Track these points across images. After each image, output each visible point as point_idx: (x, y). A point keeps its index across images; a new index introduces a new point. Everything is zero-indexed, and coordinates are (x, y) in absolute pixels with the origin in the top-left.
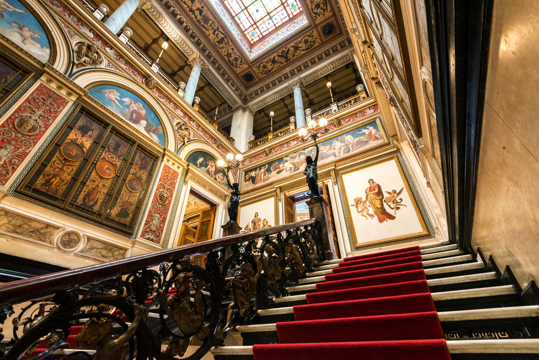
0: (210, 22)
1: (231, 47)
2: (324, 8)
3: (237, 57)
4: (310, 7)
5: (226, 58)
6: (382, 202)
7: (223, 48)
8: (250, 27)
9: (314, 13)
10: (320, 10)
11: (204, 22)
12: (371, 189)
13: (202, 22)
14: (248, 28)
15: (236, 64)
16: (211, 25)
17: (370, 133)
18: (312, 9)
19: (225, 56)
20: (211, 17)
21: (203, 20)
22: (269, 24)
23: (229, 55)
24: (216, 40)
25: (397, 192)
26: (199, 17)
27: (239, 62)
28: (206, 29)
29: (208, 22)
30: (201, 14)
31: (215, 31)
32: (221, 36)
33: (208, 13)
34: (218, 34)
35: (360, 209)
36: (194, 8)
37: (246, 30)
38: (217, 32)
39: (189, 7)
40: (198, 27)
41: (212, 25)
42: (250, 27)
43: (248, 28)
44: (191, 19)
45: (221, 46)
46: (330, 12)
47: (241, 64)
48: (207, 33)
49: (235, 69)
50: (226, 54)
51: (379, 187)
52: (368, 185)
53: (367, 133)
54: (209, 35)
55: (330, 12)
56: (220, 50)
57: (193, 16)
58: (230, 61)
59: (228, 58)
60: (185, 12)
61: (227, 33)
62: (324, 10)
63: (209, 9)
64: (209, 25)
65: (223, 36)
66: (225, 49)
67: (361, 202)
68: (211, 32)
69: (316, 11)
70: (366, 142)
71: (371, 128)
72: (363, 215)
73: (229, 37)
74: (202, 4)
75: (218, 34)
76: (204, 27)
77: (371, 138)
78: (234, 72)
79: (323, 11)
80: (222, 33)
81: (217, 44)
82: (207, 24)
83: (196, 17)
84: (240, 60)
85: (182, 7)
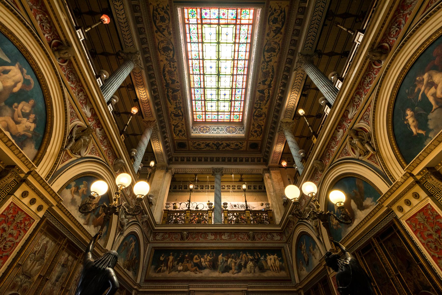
0: (264, 71)
1: (268, 38)
2: (157, 13)
3: (271, 23)
4: (171, 23)
5: (282, 30)
7: (276, 43)
8: (243, 24)
9: (168, 15)
10: (161, 12)
11: (269, 73)
13: (270, 75)
14: (245, 24)
15: (279, 15)
16: (267, 68)
18: (169, 20)
19: (281, 33)
20: (260, 73)
21: (268, 76)
22: (224, 14)
23: (278, 31)
24: (275, 54)
26: (269, 79)
27: (276, 15)
28: (273, 68)
29: (266, 72)
30: (266, 80)
31: (268, 62)
32: (267, 55)
33: (259, 77)
34: (268, 58)
36: (266, 87)
37: (249, 24)
38: (267, 60)
39: (269, 90)
40: (277, 74)
41: (265, 68)
42: (243, 24)
43: (245, 24)
44: (276, 82)
45: (276, 46)
46: (151, 4)
47: (275, 10)
48: (275, 65)
49: (287, 10)
50: (279, 35)
54: (276, 62)
55: (151, 4)
56: (280, 42)
57: (272, 82)
58: (283, 24)
59: (281, 29)
60: (274, 89)
61: (260, 53)
62: (157, 11)
63: (257, 80)
64: (268, 70)
65: (266, 53)
66: (275, 40)
68: (272, 63)
69: (166, 16)
73: (261, 49)
74: (258, 85)
75: (268, 58)
76: (273, 71)
78: (291, 7)
79: (159, 10)
80: (264, 56)
81: (277, 50)
82: (269, 71)
83: (271, 81)
84: (272, 17)
85: (273, 92)
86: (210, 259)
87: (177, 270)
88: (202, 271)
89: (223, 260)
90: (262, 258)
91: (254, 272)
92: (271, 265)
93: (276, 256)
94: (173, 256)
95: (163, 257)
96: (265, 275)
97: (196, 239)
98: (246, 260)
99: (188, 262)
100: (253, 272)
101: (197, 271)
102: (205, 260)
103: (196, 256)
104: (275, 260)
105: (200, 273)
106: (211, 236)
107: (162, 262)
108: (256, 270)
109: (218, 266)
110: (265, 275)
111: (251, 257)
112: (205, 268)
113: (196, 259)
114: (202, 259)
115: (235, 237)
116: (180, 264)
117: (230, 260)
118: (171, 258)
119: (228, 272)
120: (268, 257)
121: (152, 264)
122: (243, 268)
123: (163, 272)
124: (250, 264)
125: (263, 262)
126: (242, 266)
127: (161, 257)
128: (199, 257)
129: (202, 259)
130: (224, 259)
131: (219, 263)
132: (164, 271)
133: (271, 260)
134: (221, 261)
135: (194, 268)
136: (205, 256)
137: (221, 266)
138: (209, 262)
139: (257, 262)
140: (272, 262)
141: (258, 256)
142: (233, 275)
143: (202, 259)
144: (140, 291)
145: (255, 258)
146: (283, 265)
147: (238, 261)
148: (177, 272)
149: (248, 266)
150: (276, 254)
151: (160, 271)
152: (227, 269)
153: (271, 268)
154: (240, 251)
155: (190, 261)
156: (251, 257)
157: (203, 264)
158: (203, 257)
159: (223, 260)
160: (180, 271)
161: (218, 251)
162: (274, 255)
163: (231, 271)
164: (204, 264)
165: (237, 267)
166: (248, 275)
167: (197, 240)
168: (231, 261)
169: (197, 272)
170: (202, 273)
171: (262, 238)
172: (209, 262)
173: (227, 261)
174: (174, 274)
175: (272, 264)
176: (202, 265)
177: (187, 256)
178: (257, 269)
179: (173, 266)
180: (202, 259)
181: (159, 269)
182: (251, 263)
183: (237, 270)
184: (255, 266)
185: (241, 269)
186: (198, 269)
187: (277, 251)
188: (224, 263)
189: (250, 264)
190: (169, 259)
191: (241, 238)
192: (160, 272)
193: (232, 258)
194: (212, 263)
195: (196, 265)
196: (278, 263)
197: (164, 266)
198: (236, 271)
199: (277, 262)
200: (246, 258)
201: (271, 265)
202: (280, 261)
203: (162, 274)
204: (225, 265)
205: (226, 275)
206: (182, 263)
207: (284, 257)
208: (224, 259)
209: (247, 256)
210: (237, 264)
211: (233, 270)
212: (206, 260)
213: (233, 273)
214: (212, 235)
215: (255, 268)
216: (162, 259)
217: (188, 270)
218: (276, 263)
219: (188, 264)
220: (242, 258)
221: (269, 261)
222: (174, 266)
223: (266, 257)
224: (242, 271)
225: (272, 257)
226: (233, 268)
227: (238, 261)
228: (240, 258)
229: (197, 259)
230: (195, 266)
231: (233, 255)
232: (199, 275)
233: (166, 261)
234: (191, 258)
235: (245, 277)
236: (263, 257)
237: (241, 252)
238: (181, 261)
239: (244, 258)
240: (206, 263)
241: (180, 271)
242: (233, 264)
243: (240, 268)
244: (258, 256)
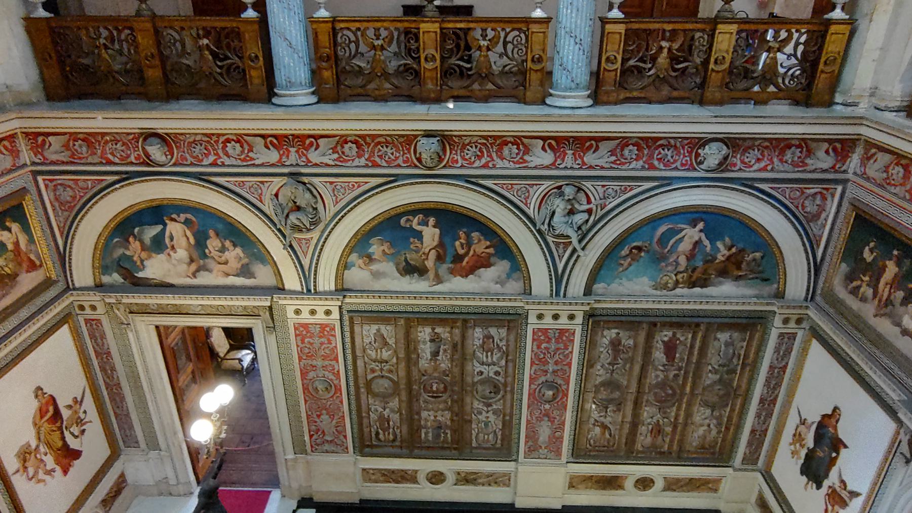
6: (62, 433)
12: (42, 412)
17: (17, 244)
25: (79, 399)
35: (31, 471)
51: (53, 399)
52: (34, 405)
53: (10, 247)
67: (30, 453)
70: (13, 277)
71: (15, 227)
72: (39, 481)
77: (20, 264)
94: (899, 264)
95: (871, 251)
123: (861, 300)
132: (863, 300)
216: (868, 256)
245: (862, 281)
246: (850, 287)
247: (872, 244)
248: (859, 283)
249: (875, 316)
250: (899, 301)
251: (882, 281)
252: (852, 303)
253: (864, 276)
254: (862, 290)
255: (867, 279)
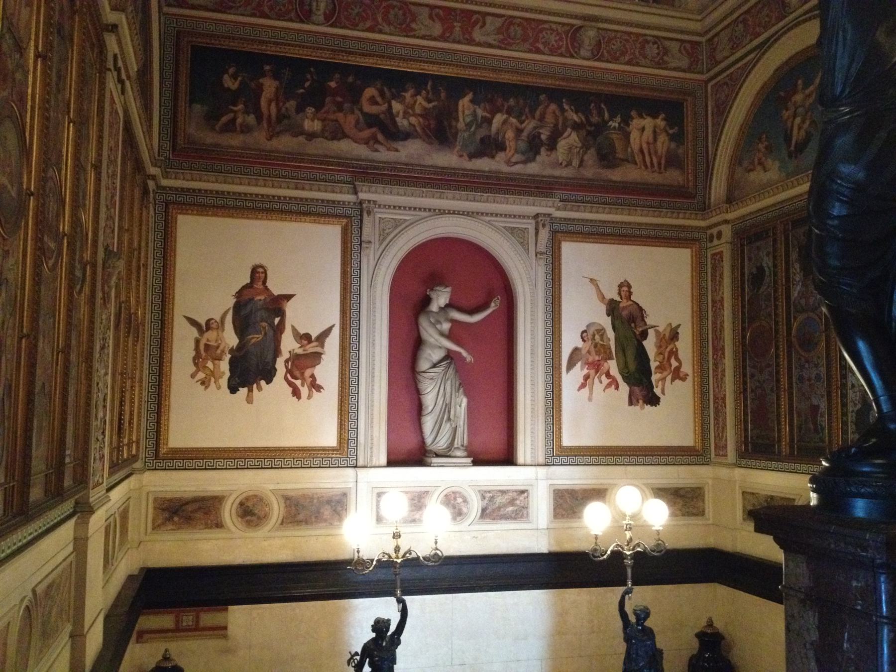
86: (425, 109)
87: (302, 133)
88: (399, 145)
89: (474, 114)
90: (614, 124)
91: (581, 164)
92: (641, 151)
93: (660, 122)
95: (234, 77)
96: (616, 175)
97: (368, 24)
98: (556, 125)
99: (340, 109)
100: (575, 162)
101: (377, 141)
102: (409, 108)
103: (370, 92)
104: (655, 132)
105: (389, 149)
106: (428, 22)
107: (234, 98)
108: (586, 158)
109: (455, 135)
110: (616, 175)
111: (575, 118)
112: (406, 136)
113: (373, 101)
114: (397, 106)
115: (525, 40)
116: (310, 110)
117: (499, 118)
118: (269, 86)
119: (493, 157)
120: (636, 122)
121: (192, 101)
122: (543, 150)
123: (242, 132)
124: (570, 140)
125: (614, 136)
126: (542, 143)
127: (226, 77)
128: (382, 94)
129: (397, 106)
130: (480, 112)
131: (461, 125)
132: (246, 129)
133: (643, 130)
134: (468, 120)
135: (367, 133)
136: (408, 95)
137: (466, 135)
138: (421, 116)
139: (593, 134)
140: (645, 138)
141: (600, 113)
142: (505, 169)
143: (394, 103)
144: (164, 188)
145: (591, 124)
146: (680, 151)
147: (529, 125)
148: (301, 139)
149: (562, 144)
150: (662, 116)
151: (230, 127)
152: (490, 146)
153: (638, 159)
154: (537, 90)
155: (346, 106)
156: (575, 118)
157: (402, 123)
158: (397, 97)
159: (474, 114)
160: (311, 136)
161: (456, 87)
162: (655, 116)
163: (501, 156)
164: (405, 122)
165: (522, 145)
166: (557, 172)
167: (371, 30)
168: (505, 122)
169: (377, 146)
170: (397, 150)
171: (623, 54)
172: (421, 116)
173: (489, 121)
174: (286, 143)
175: (645, 146)
176: (395, 123)
177: (333, 84)
178: (590, 157)
179: (281, 117)
180: (394, 103)
181: (224, 119)
182: (574, 136)
183: (523, 153)
184: (586, 147)
185: (538, 153)
186: (380, 137)
187: (669, 107)
188: (479, 126)
189: (570, 140)
190: (260, 88)
191: (546, 44)
192: (234, 131)
193: (509, 112)
194: (433, 123)
195: (372, 121)
196: (663, 144)
197: (247, 113)
198: (517, 157)
199: (662, 138)
200: (557, 120)
201: (641, 151)
202: (672, 138)
203: (242, 137)
204: (482, 133)
205: (483, 164)
206: (318, 108)
207: (689, 128)
208: (480, 112)
209: (563, 110)
210: (525, 134)
211: (509, 152)
212: (412, 107)
213: (508, 163)
214: (431, 17)
215: (585, 153)
216: (229, 83)
217: (345, 136)
218: (659, 144)
219: (340, 116)
220: (542, 118)
221: (634, 136)
222: (289, 117)
223: (626, 120)
224: (538, 158)
225: (648, 122)
226: (510, 144)
227: (529, 125)
228: (538, 114)
229: (377, 103)
230: (370, 126)
231: (512, 102)
232: (384, 155)
233: (250, 97)
234: (354, 95)
235: (549, 177)
236: (618, 119)
237: (542, 97)
238: (315, 99)
239: (549, 118)
240: (413, 120)
241: (311, 136)
242: (510, 134)
243: (533, 147)
244: (600, 113)
245: (235, 112)
246: (217, 128)
247: (231, 70)
248: (232, 115)
249: (270, 139)
250: (293, 110)
251: (263, 103)
252: (235, 141)
253: (235, 105)
254: (239, 121)
255: (241, 107)
